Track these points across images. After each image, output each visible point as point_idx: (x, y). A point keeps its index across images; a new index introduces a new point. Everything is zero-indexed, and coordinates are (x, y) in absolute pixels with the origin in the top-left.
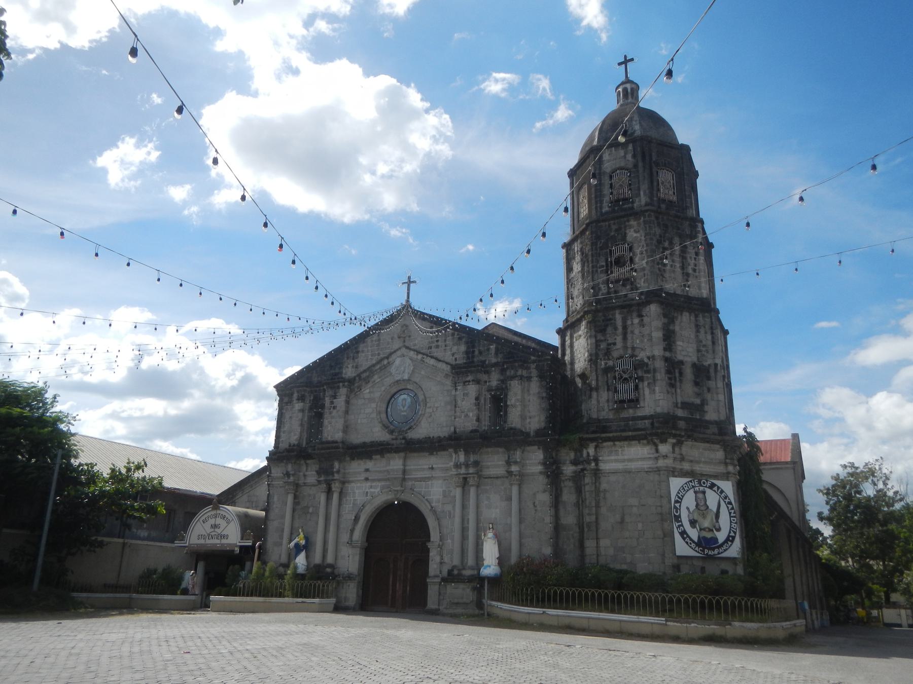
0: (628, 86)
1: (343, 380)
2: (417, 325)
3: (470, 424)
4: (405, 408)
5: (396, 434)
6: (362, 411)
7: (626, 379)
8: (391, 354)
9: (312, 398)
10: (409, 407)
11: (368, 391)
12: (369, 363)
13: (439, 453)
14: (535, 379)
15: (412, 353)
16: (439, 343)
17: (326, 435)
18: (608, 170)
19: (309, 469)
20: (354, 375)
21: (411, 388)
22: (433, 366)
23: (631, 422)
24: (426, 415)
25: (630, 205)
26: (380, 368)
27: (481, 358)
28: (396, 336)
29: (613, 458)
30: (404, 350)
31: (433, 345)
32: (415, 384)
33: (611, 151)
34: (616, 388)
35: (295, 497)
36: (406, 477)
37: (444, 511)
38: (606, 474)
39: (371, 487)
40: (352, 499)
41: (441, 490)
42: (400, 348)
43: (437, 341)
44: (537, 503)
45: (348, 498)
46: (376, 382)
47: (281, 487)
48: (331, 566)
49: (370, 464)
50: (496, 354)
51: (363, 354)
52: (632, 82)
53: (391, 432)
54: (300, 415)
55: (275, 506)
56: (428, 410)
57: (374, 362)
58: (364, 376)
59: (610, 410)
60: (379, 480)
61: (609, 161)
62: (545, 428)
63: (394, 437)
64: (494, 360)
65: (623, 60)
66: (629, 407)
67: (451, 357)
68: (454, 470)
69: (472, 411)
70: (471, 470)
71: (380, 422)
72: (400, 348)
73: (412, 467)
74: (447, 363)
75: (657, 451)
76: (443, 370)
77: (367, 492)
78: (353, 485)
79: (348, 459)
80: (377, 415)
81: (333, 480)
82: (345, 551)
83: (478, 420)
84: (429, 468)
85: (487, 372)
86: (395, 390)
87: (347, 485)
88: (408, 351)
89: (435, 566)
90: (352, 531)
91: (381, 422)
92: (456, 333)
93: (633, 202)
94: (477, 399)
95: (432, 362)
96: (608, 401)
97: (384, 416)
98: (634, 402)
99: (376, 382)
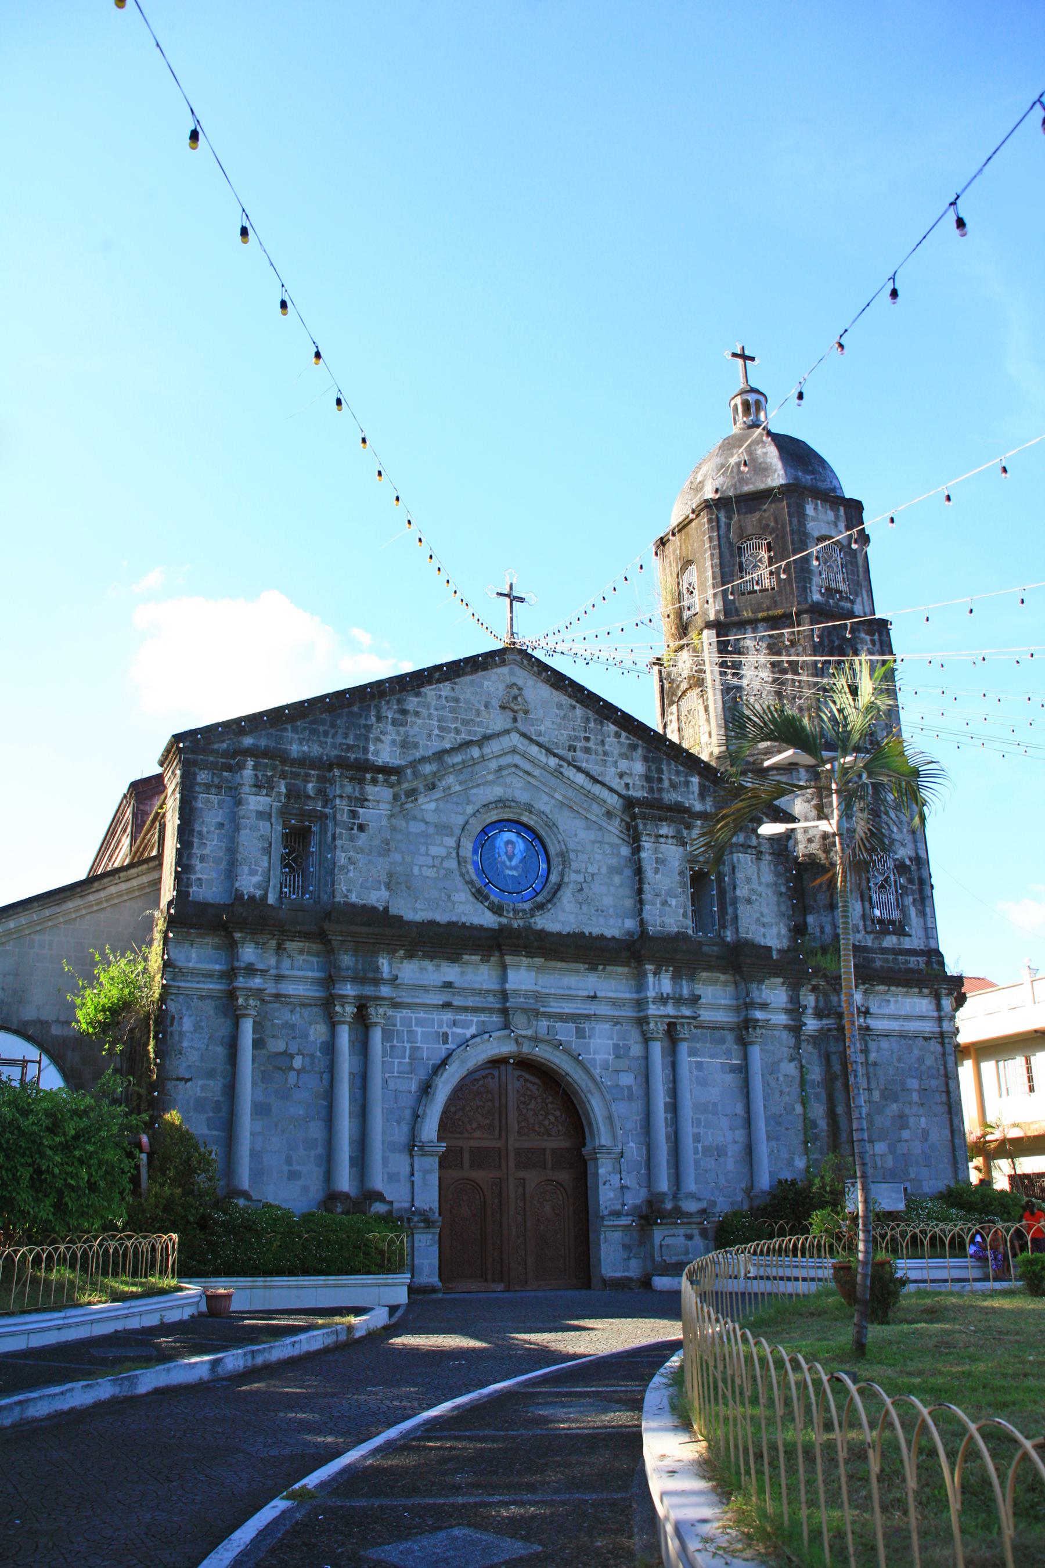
0: (762, 399)
1: (387, 770)
2: (538, 692)
3: (672, 921)
4: (514, 863)
5: (511, 915)
6: (423, 850)
7: (882, 886)
8: (487, 738)
9: (283, 790)
10: (523, 860)
11: (433, 806)
12: (436, 745)
13: (609, 968)
14: (767, 857)
15: (534, 750)
16: (591, 744)
17: (344, 889)
18: (816, 534)
19: (286, 963)
20: (396, 762)
21: (532, 823)
22: (582, 787)
23: (900, 957)
24: (571, 886)
25: (848, 605)
26: (463, 762)
27: (674, 795)
28: (495, 703)
29: (887, 1011)
30: (515, 739)
31: (579, 745)
32: (544, 817)
33: (816, 505)
34: (870, 898)
35: (258, 1027)
37: (617, 1085)
38: (875, 1037)
39: (455, 1023)
40: (408, 1045)
41: (611, 1042)
42: (507, 732)
43: (587, 739)
44: (781, 1079)
45: (395, 1042)
46: (453, 790)
47: (202, 998)
48: (379, 1197)
49: (450, 972)
50: (702, 796)
51: (419, 722)
52: (757, 391)
53: (497, 910)
54: (264, 826)
55: (185, 1044)
56: (574, 877)
57: (448, 746)
58: (427, 769)
59: (867, 932)
60: (475, 1010)
61: (814, 519)
62: (789, 950)
63: (504, 920)
64: (698, 807)
65: (739, 352)
66: (894, 933)
67: (617, 780)
68: (654, 1007)
69: (676, 897)
70: (687, 1012)
71: (467, 883)
72: (507, 732)
73: (553, 991)
74: (611, 790)
75: (939, 1007)
76: (605, 802)
77: (445, 1035)
78: (406, 1013)
79: (401, 953)
80: (459, 864)
81: (377, 998)
82: (400, 1163)
83: (685, 915)
85: (689, 827)
86: (494, 818)
88: (526, 742)
89: (612, 1195)
90: (417, 1117)
91: (471, 883)
92: (624, 734)
93: (852, 602)
94: (681, 873)
95: (580, 779)
96: (864, 917)
97: (471, 868)
98: (900, 929)
99: (453, 790)
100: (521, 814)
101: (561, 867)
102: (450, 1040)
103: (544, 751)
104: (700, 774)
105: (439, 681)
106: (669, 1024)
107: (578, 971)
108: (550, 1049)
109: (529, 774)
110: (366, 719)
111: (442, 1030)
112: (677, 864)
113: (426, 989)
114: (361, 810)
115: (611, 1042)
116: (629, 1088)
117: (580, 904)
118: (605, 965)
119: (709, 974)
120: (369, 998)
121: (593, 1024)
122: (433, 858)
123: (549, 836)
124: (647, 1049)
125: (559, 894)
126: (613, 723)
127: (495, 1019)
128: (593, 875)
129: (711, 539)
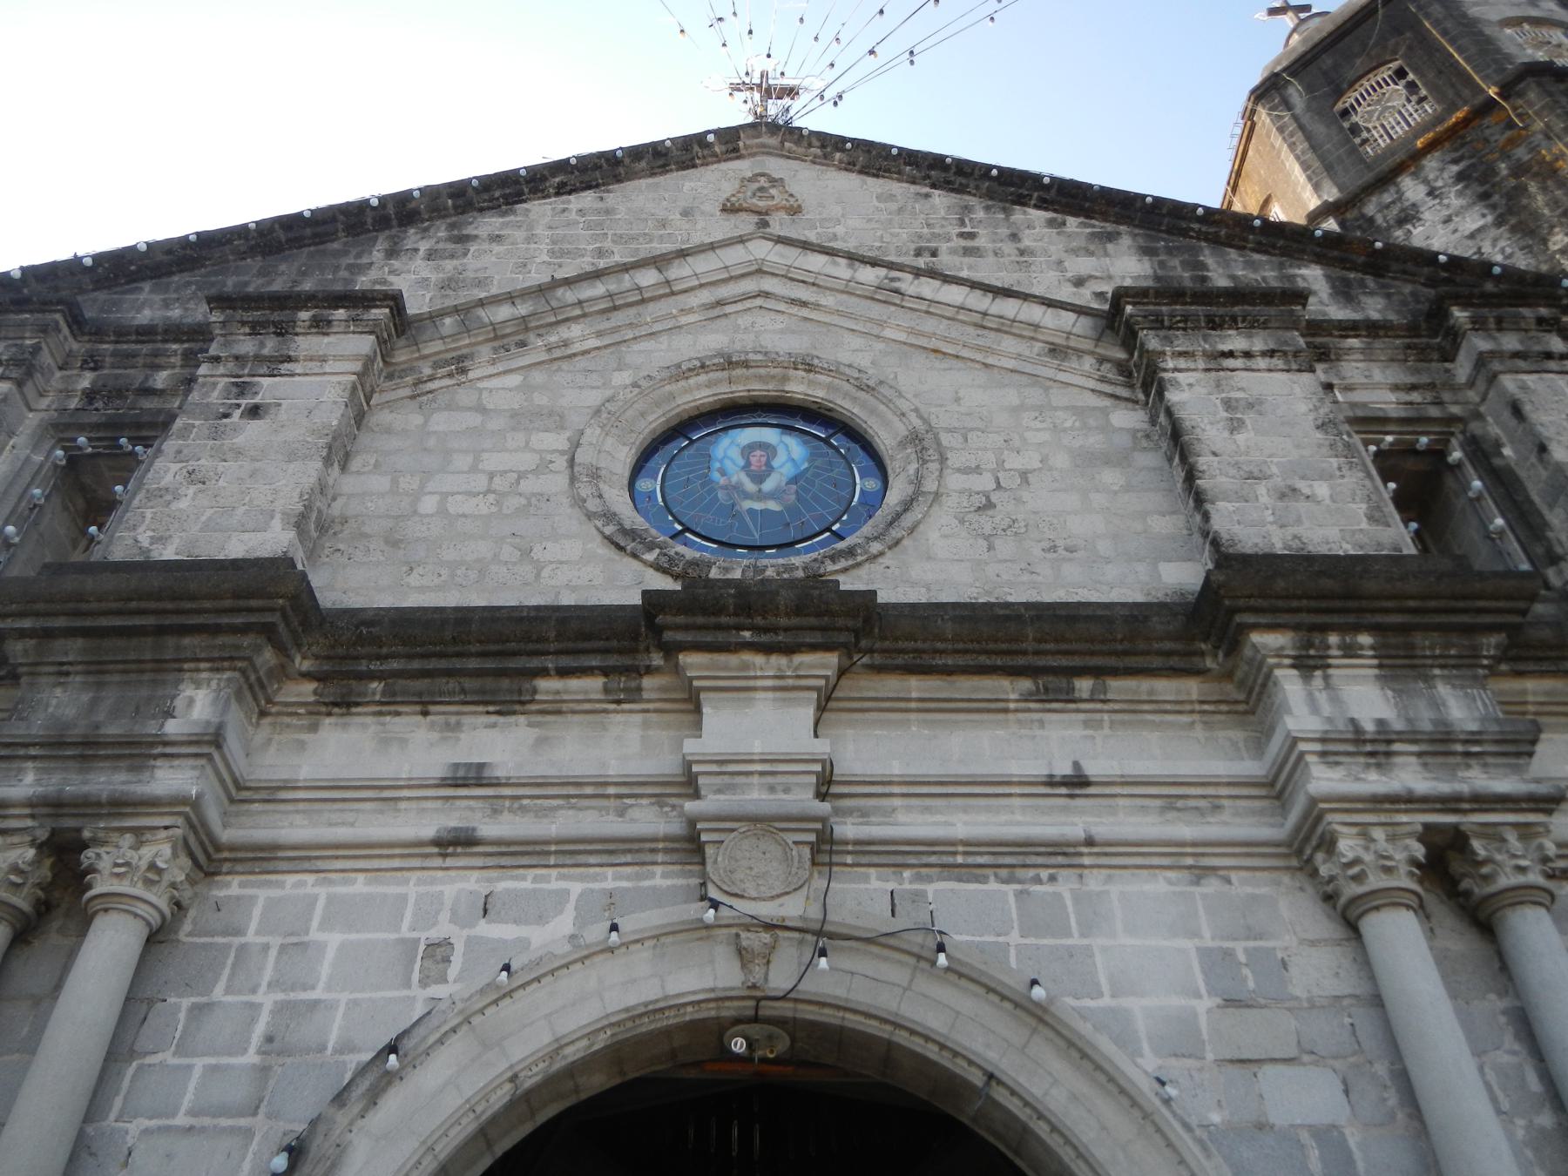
6: (462, 462)
11: (515, 380)
13: (1119, 687)
21: (819, 394)
24: (951, 502)
36: (847, 829)
37: (1262, 1126)
45: (218, 993)
46: (577, 348)
56: (954, 481)
69: (1324, 476)
71: (590, 516)
73: (896, 769)
74: (1050, 303)
78: (295, 886)
84: (1051, 782)
87: (232, 887)
92: (1072, 222)
100: (785, 379)
101: (914, 466)
102: (453, 971)
103: (843, 261)
104: (1319, 259)
105: (562, 190)
106: (1428, 834)
107: (995, 707)
108: (895, 972)
109: (804, 304)
110: (359, 256)
111: (435, 934)
112: (1303, 407)
113: (384, 793)
114: (266, 381)
115: (1189, 944)
116: (1327, 1135)
117: (987, 538)
118: (1098, 672)
119: (1548, 684)
120: (88, 806)
121: (1094, 881)
122: (491, 476)
123: (873, 411)
124: (1364, 962)
125: (908, 520)
126: (1037, 207)
127: (659, 881)
128: (1024, 476)
129: (1281, 130)
